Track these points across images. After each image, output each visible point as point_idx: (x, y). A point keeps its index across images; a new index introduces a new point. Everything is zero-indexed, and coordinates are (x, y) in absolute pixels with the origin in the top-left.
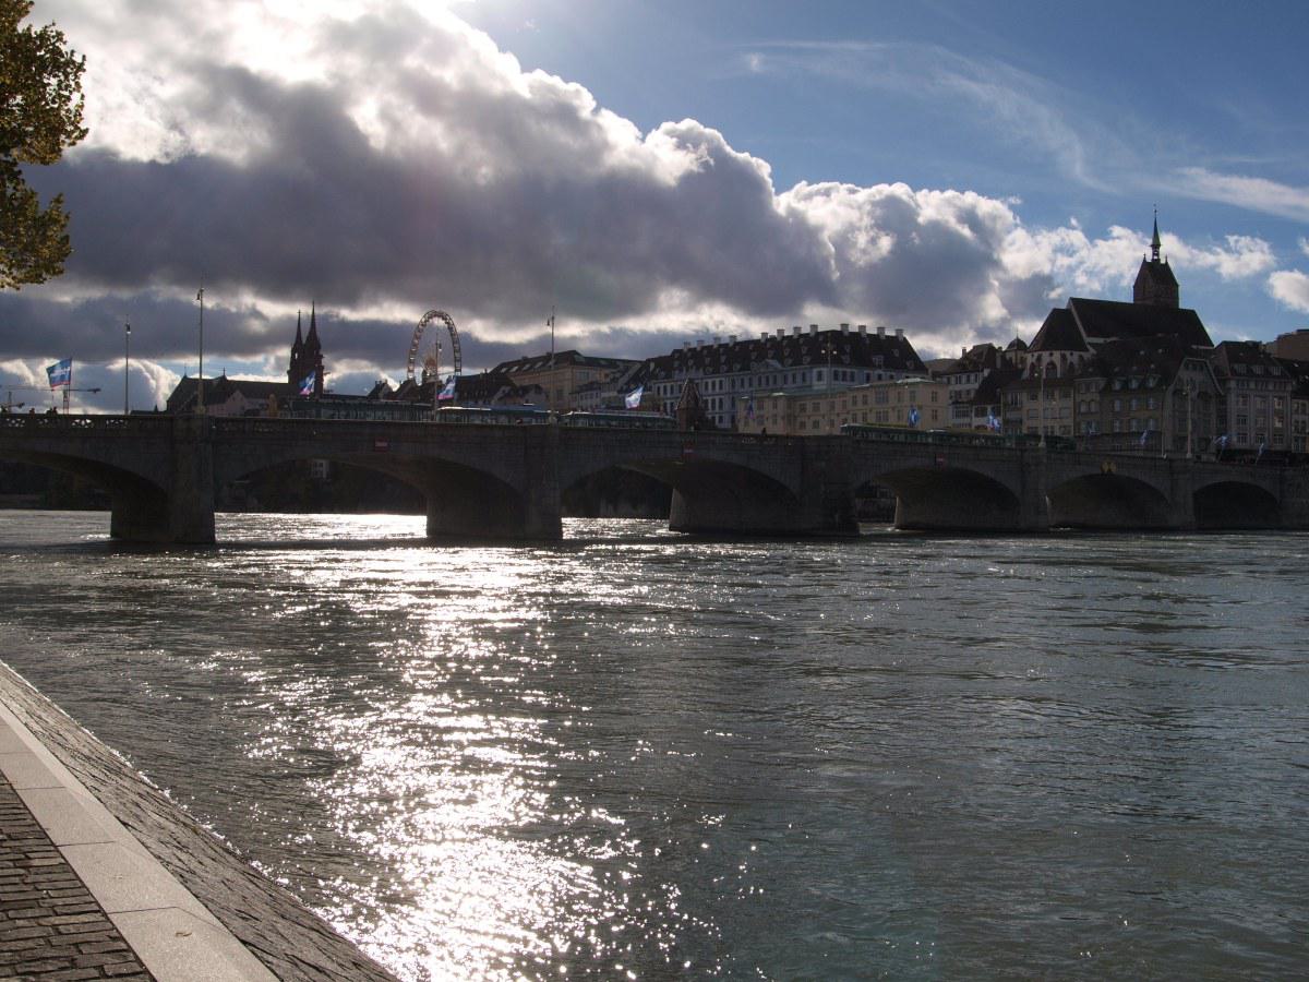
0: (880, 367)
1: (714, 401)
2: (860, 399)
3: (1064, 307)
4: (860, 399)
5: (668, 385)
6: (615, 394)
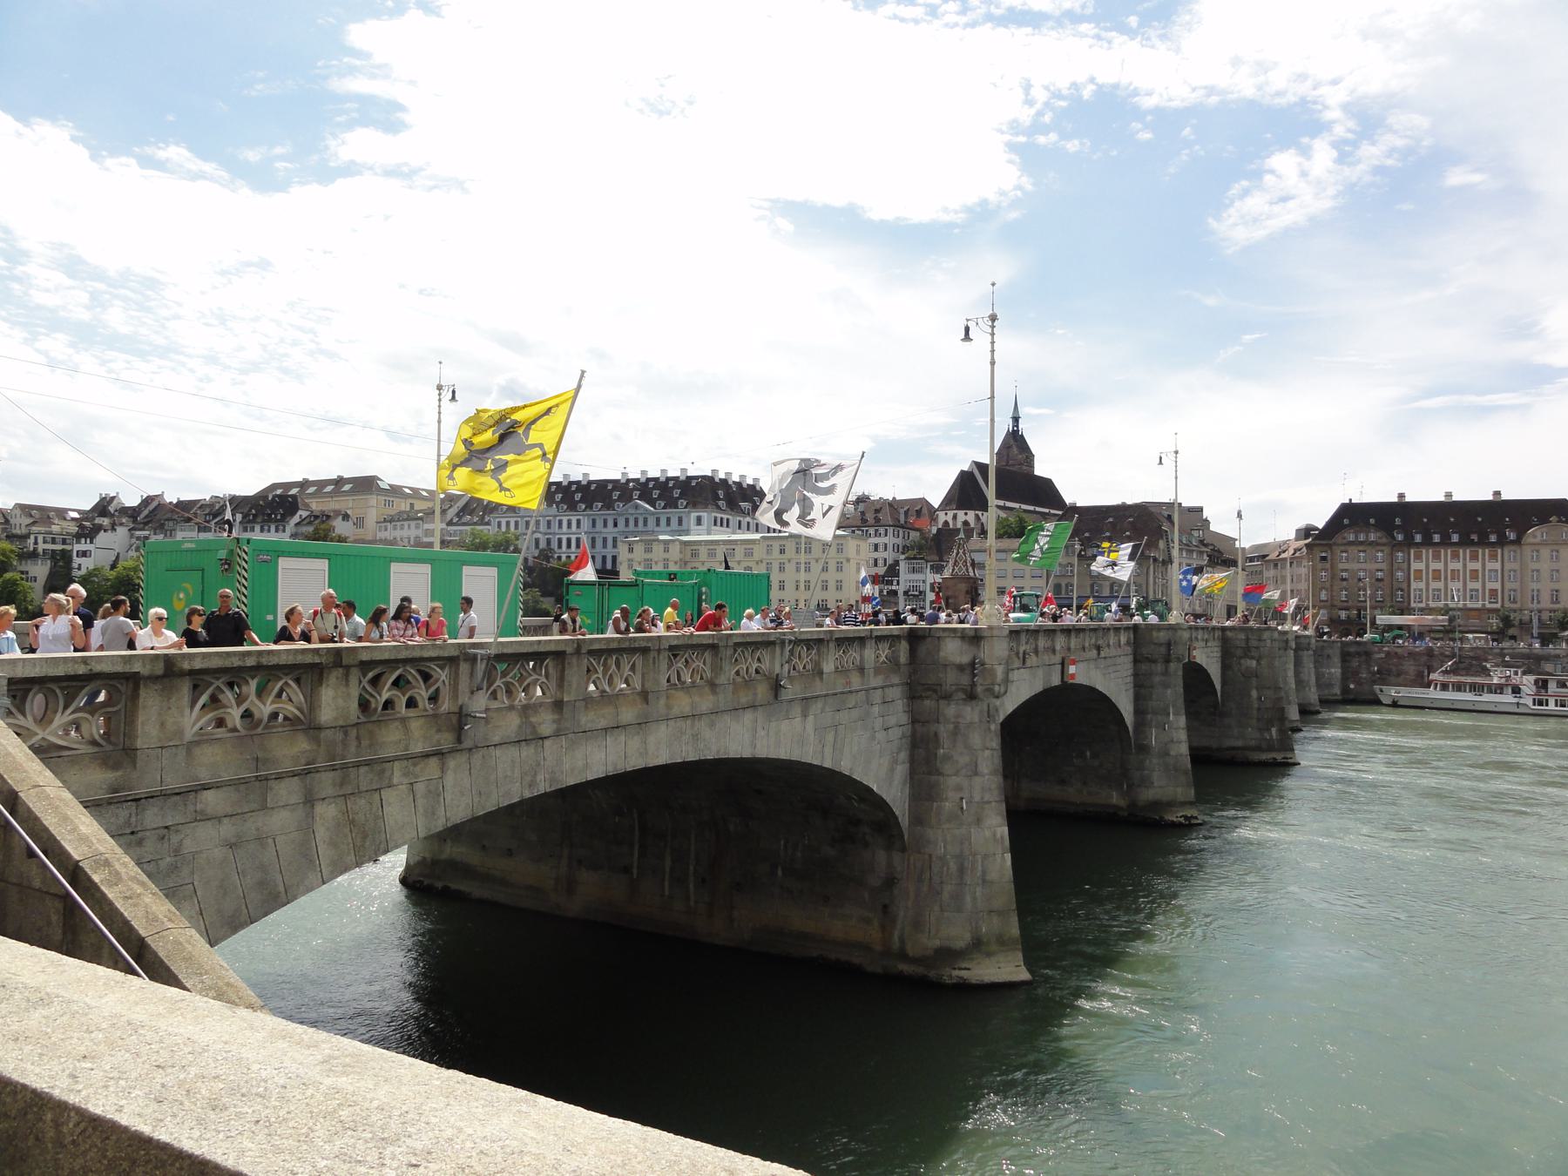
1: (569, 541)
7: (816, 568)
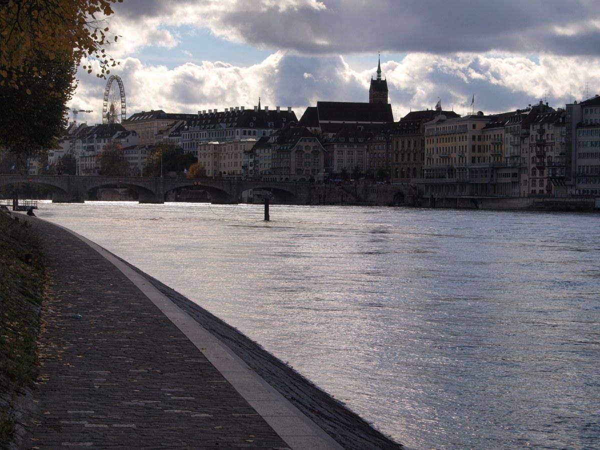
0: (271, 128)
5: (187, 133)
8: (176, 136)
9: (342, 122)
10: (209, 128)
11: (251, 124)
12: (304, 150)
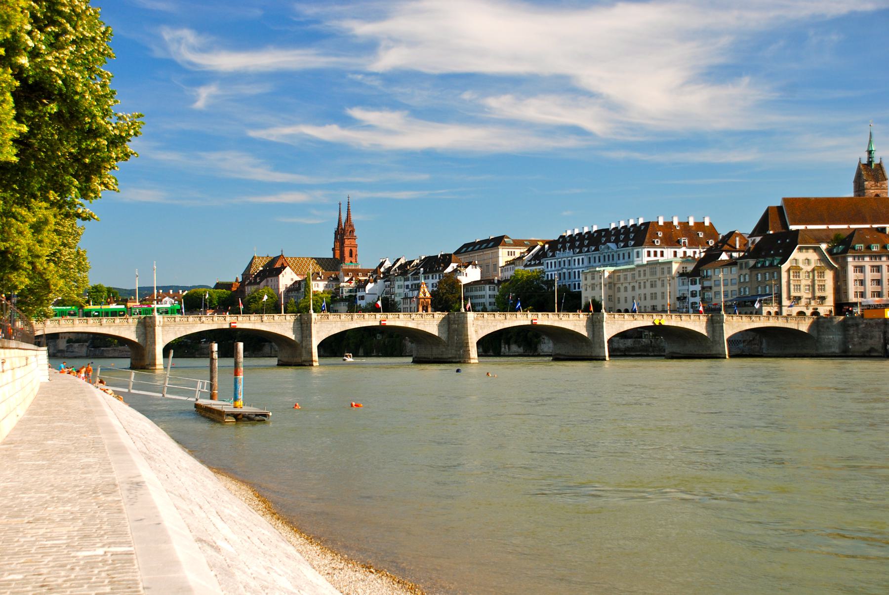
0: (685, 245)
2: (642, 273)
3: (779, 205)
4: (642, 273)
5: (553, 261)
6: (522, 267)
7: (659, 283)
8: (535, 265)
9: (824, 227)
10: (588, 251)
11: (658, 242)
12: (801, 265)
